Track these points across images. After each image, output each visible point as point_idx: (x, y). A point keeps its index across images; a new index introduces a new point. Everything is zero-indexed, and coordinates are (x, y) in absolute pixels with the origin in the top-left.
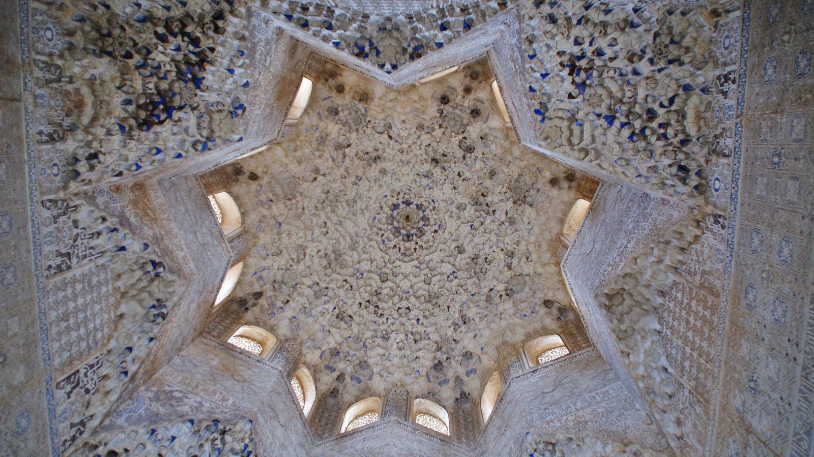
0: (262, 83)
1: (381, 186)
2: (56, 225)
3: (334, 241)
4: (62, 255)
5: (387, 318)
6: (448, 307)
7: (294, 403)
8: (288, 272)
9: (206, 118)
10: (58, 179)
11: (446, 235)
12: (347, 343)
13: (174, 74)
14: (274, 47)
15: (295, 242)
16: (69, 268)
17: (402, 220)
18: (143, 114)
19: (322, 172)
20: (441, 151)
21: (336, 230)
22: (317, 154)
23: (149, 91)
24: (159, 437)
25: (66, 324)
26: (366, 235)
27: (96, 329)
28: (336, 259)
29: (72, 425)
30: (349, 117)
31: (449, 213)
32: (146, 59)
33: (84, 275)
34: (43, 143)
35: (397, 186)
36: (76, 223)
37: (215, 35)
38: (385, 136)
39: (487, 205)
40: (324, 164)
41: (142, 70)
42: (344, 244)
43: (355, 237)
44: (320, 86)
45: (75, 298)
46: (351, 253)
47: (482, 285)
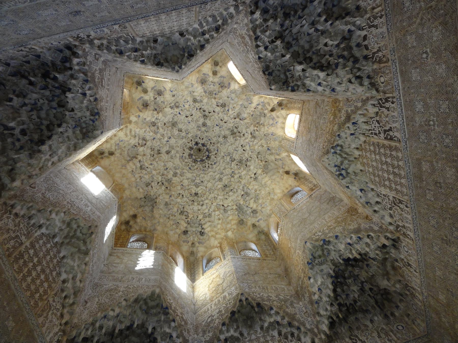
0: (301, 270)
2: (403, 223)
5: (197, 109)
6: (165, 124)
8: (258, 121)
11: (178, 155)
13: (346, 275)
14: (299, 289)
16: (394, 197)
19: (252, 179)
20: (196, 204)
22: (258, 192)
24: (329, 87)
29: (388, 109)
32: (362, 286)
33: (385, 186)
36: (391, 216)
37: (332, 316)
42: (231, 139)
46: (226, 133)
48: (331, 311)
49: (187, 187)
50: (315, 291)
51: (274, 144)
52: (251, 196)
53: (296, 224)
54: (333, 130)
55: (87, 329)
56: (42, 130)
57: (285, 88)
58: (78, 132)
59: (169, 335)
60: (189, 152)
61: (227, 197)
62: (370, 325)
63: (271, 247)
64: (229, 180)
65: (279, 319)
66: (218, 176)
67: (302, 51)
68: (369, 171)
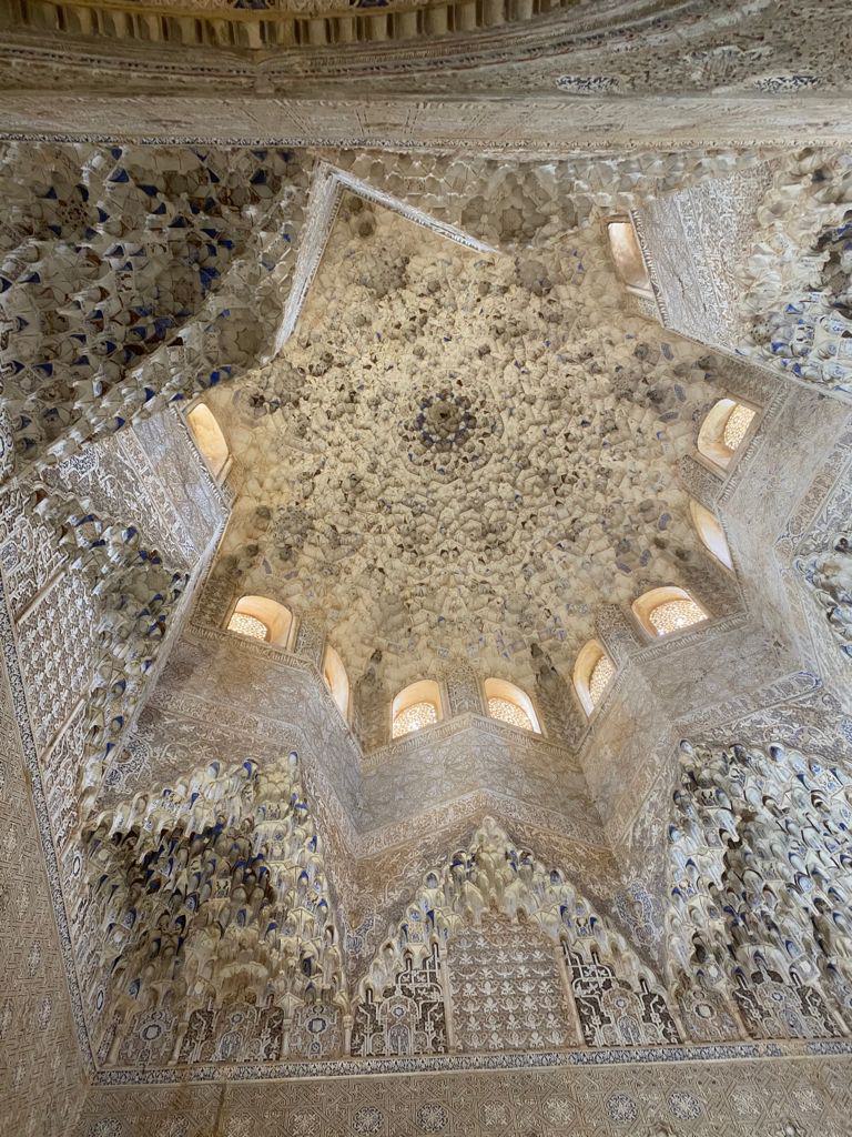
1: (395, 466)
2: (385, 1026)
3: (468, 539)
4: (424, 1019)
7: (680, 640)
9: (267, 803)
10: (329, 1022)
11: (464, 371)
12: (611, 527)
13: (208, 853)
14: (168, 722)
15: (464, 599)
16: (442, 1007)
17: (447, 425)
18: (259, 893)
19: (371, 562)
20: (336, 395)
21: (453, 534)
22: (343, 576)
23: (229, 886)
24: (685, 884)
25: (511, 1018)
26: (462, 484)
27: (530, 963)
28: (495, 532)
29: (647, 1018)
30: (293, 528)
31: (431, 368)
33: (458, 981)
34: (281, 1047)
35: (394, 444)
36: (388, 992)
39: (413, 319)
40: (359, 563)
41: (201, 900)
43: (466, 503)
44: (247, 584)
45: (482, 998)
47: (534, 328)
52: (330, 552)
59: (154, 388)
60: (456, 395)
66: (383, 463)
67: (753, 829)
68: (477, 936)
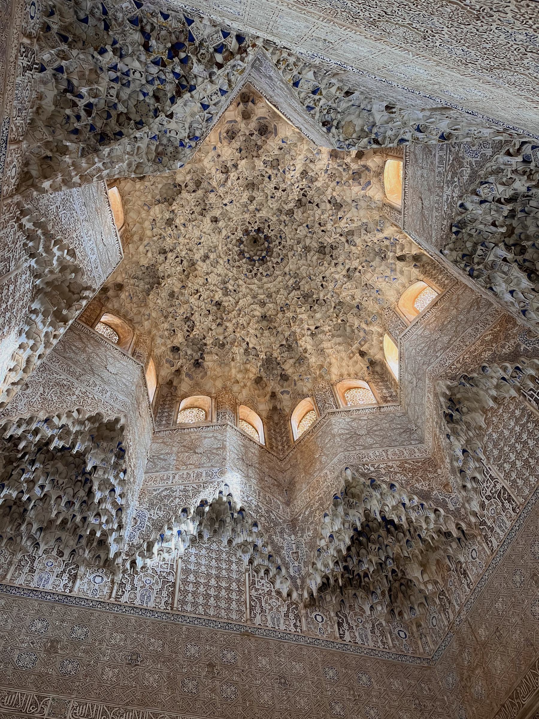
0: (317, 497)
2: (493, 525)
6: (239, 178)
8: (368, 259)
10: (476, 548)
14: (300, 518)
19: (309, 332)
20: (210, 317)
22: (307, 355)
24: (522, 304)
26: (292, 253)
30: (274, 366)
32: (385, 562)
33: (500, 467)
36: (482, 506)
37: (330, 576)
38: (251, 346)
42: (313, 257)
43: (304, 255)
44: (287, 410)
47: (202, 195)
48: (333, 571)
49: (212, 288)
50: (324, 535)
51: (371, 306)
53: (342, 434)
54: (480, 355)
55: (19, 426)
56: (109, 116)
57: (462, 265)
58: (153, 148)
59: (111, 488)
60: (242, 236)
61: (259, 335)
62: (368, 612)
63: (282, 438)
64: (274, 313)
65: (260, 543)
66: (262, 297)
67: (521, 231)
